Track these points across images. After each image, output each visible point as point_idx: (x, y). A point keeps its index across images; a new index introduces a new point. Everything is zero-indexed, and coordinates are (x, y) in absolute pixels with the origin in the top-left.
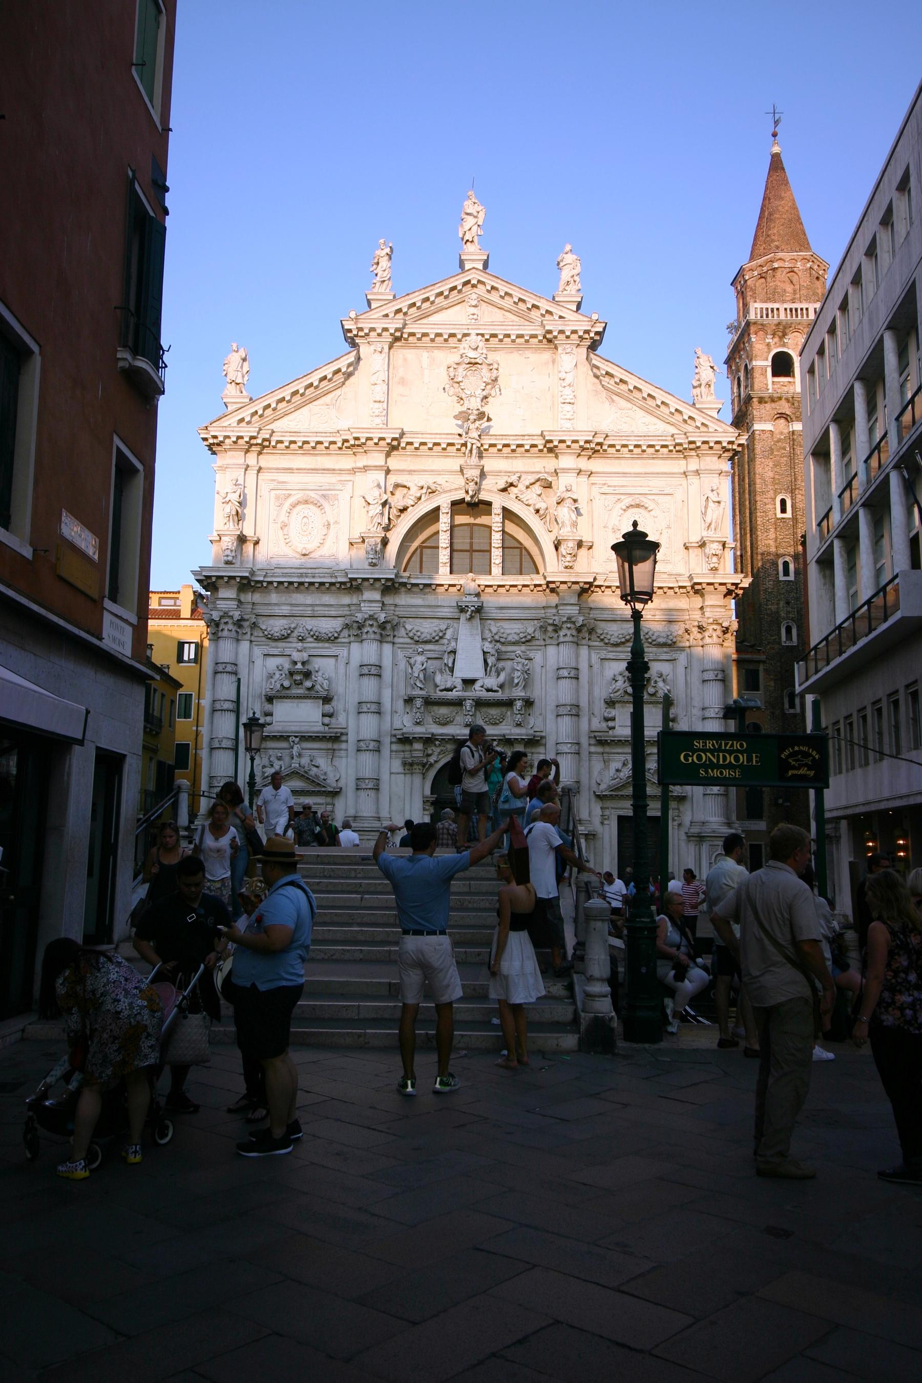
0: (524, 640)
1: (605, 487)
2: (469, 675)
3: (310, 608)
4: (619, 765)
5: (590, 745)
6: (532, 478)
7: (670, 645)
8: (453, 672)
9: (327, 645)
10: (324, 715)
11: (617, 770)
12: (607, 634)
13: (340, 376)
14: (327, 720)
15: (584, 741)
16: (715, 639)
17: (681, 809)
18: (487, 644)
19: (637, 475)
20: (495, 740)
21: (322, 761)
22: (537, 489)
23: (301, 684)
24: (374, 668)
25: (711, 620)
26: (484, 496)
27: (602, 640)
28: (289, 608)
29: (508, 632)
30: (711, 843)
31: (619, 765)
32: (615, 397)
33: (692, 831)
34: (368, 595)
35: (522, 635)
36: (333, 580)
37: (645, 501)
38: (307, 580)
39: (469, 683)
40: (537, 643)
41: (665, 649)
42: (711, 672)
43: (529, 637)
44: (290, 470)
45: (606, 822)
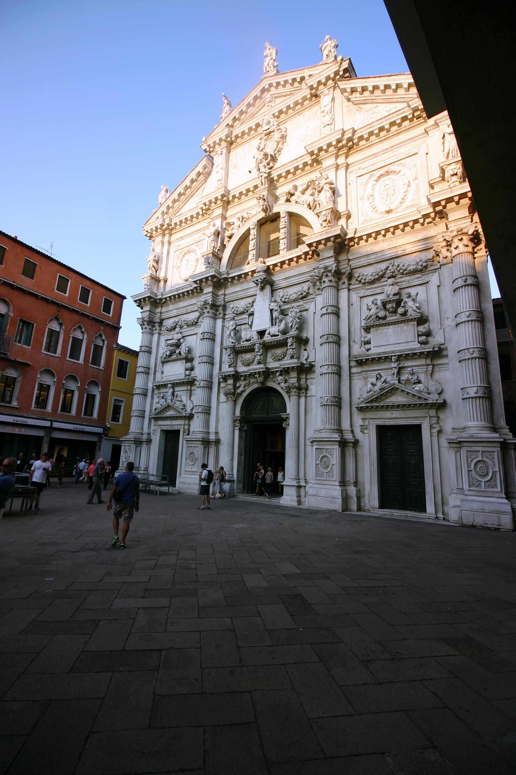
0: (301, 296)
1: (360, 171)
2: (261, 328)
3: (185, 309)
4: (374, 380)
5: (350, 367)
6: (305, 186)
7: (421, 271)
8: (251, 326)
9: (193, 328)
10: (186, 370)
11: (373, 385)
12: (363, 275)
13: (202, 177)
14: (188, 372)
15: (345, 364)
16: (462, 249)
17: (441, 416)
18: (272, 304)
19: (385, 151)
20: (277, 371)
21: (184, 398)
22: (309, 192)
23: (175, 352)
24: (206, 334)
25: (455, 233)
26: (275, 210)
27: (360, 282)
28: (176, 311)
29: (289, 294)
30: (469, 449)
31: (374, 380)
32: (362, 106)
33: (452, 437)
34: (206, 291)
35: (299, 293)
36: (192, 288)
37: (392, 168)
38: (180, 292)
39: (261, 333)
40: (312, 297)
41: (417, 276)
42: (460, 280)
43: (305, 294)
44: (182, 238)
45: (366, 431)
